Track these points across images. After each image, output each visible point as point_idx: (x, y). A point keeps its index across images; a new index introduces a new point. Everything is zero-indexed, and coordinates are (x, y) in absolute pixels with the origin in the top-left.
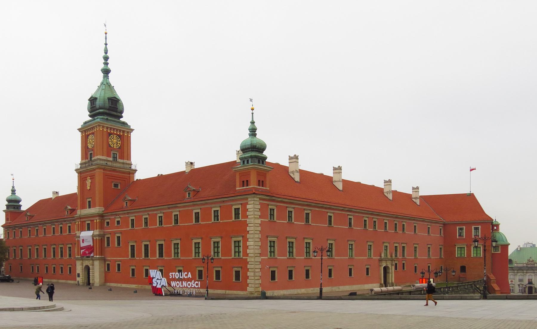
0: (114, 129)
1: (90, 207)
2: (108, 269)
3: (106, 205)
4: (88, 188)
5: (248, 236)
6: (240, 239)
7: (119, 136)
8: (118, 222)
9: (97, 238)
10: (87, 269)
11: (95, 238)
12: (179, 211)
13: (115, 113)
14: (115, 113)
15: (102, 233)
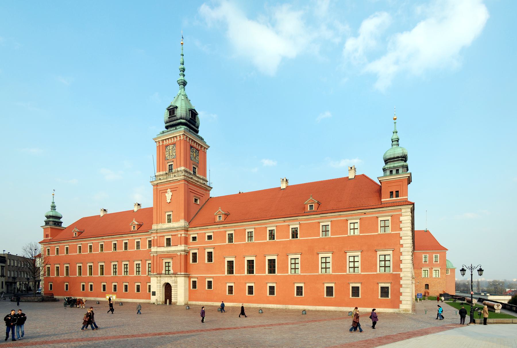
0: (195, 142)
1: (169, 221)
2: (194, 286)
3: (190, 219)
4: (169, 201)
5: (402, 250)
6: (391, 252)
7: (197, 150)
8: (210, 237)
9: (183, 253)
10: (168, 287)
11: (179, 254)
12: (300, 224)
13: (193, 126)
14: (193, 126)
15: (187, 248)
